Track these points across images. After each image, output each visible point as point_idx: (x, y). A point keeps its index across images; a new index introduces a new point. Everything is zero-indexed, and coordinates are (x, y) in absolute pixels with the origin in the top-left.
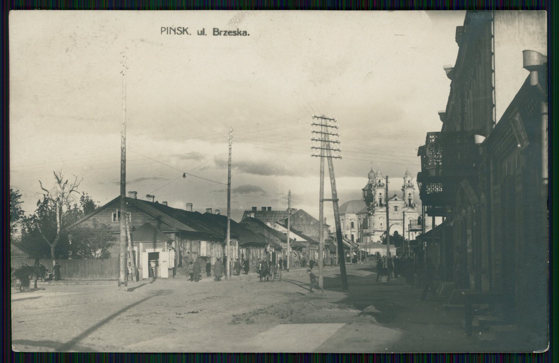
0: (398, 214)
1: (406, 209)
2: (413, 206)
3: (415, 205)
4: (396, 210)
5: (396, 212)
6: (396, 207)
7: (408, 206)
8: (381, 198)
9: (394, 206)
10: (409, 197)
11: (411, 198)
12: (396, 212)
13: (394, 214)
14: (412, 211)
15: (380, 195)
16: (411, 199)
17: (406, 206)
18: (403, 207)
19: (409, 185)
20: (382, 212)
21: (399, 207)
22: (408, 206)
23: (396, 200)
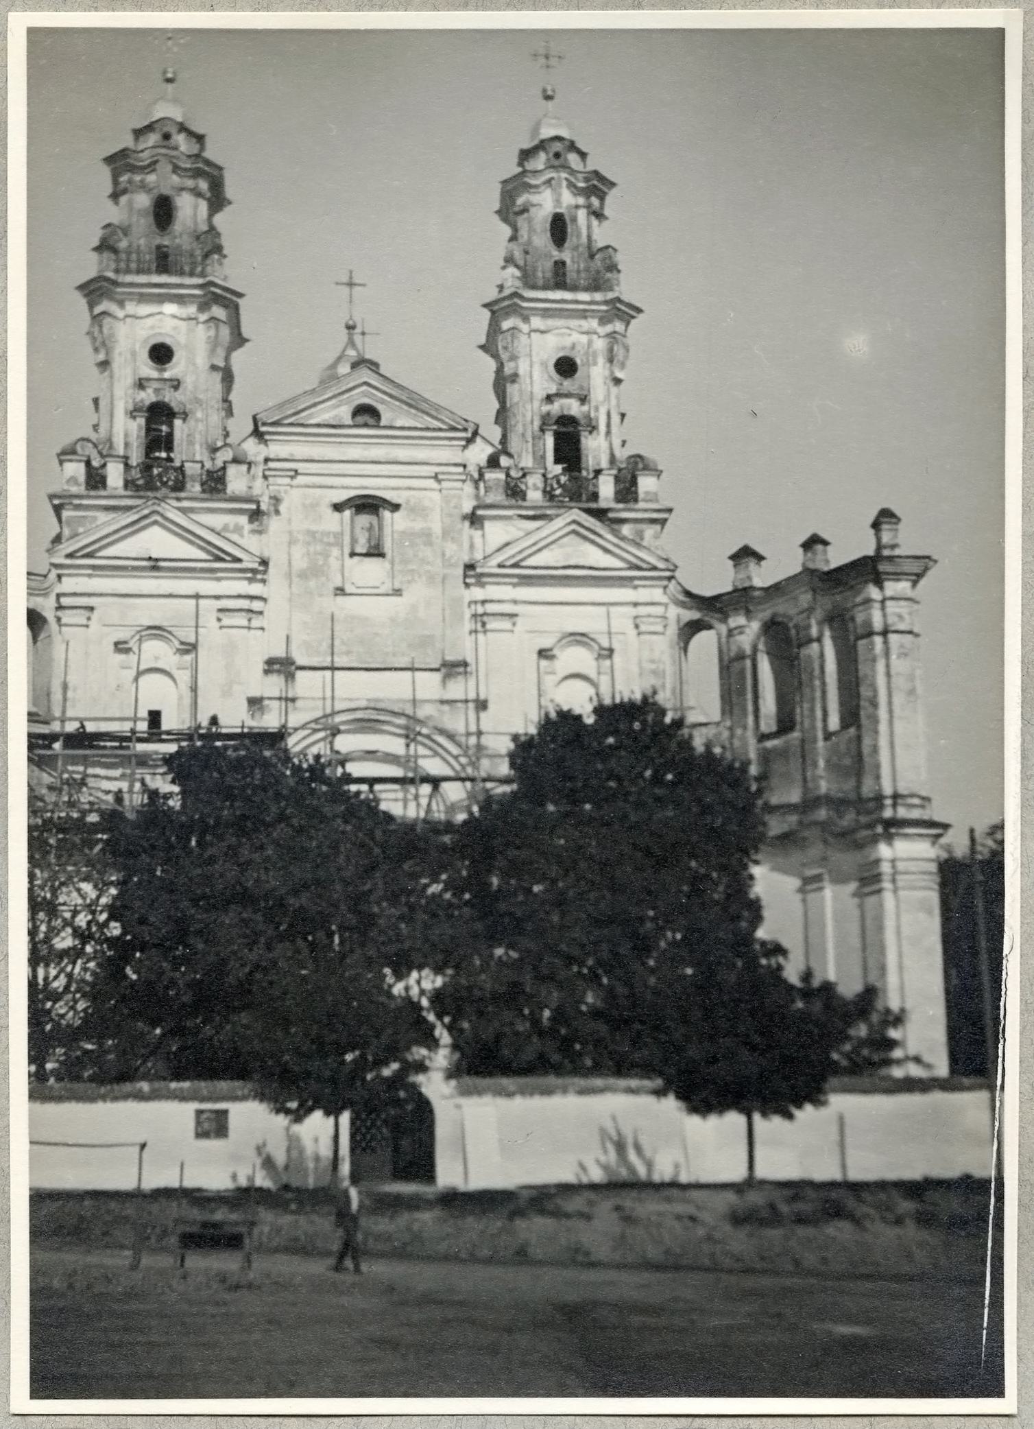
0: (398, 592)
1: (496, 532)
2: (606, 489)
3: (627, 491)
4: (376, 552)
5: (371, 572)
6: (364, 520)
7: (535, 495)
8: (172, 398)
9: (341, 496)
10: (549, 399)
11: (573, 408)
12: (373, 564)
13: (340, 591)
14: (594, 556)
15: (148, 370)
16: (593, 428)
17: (497, 497)
18: (467, 507)
19: (560, 265)
20: (154, 565)
21: (418, 511)
22: (535, 495)
23: (367, 414)
